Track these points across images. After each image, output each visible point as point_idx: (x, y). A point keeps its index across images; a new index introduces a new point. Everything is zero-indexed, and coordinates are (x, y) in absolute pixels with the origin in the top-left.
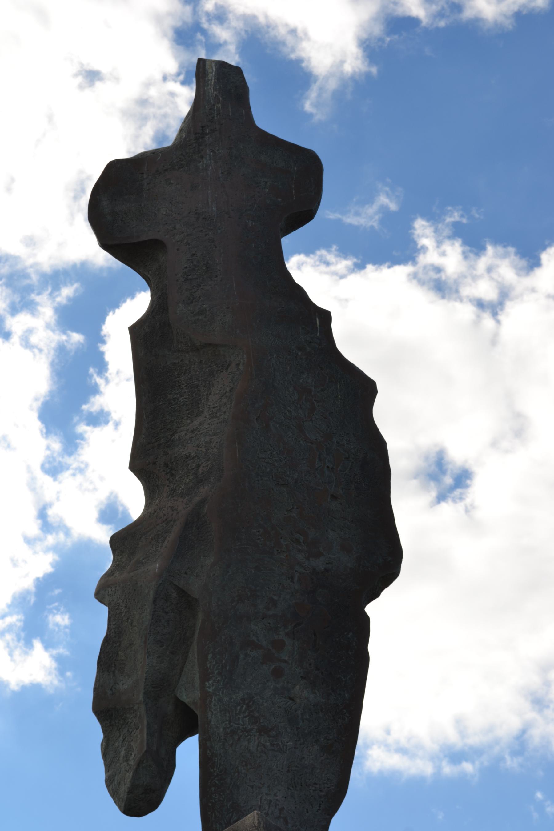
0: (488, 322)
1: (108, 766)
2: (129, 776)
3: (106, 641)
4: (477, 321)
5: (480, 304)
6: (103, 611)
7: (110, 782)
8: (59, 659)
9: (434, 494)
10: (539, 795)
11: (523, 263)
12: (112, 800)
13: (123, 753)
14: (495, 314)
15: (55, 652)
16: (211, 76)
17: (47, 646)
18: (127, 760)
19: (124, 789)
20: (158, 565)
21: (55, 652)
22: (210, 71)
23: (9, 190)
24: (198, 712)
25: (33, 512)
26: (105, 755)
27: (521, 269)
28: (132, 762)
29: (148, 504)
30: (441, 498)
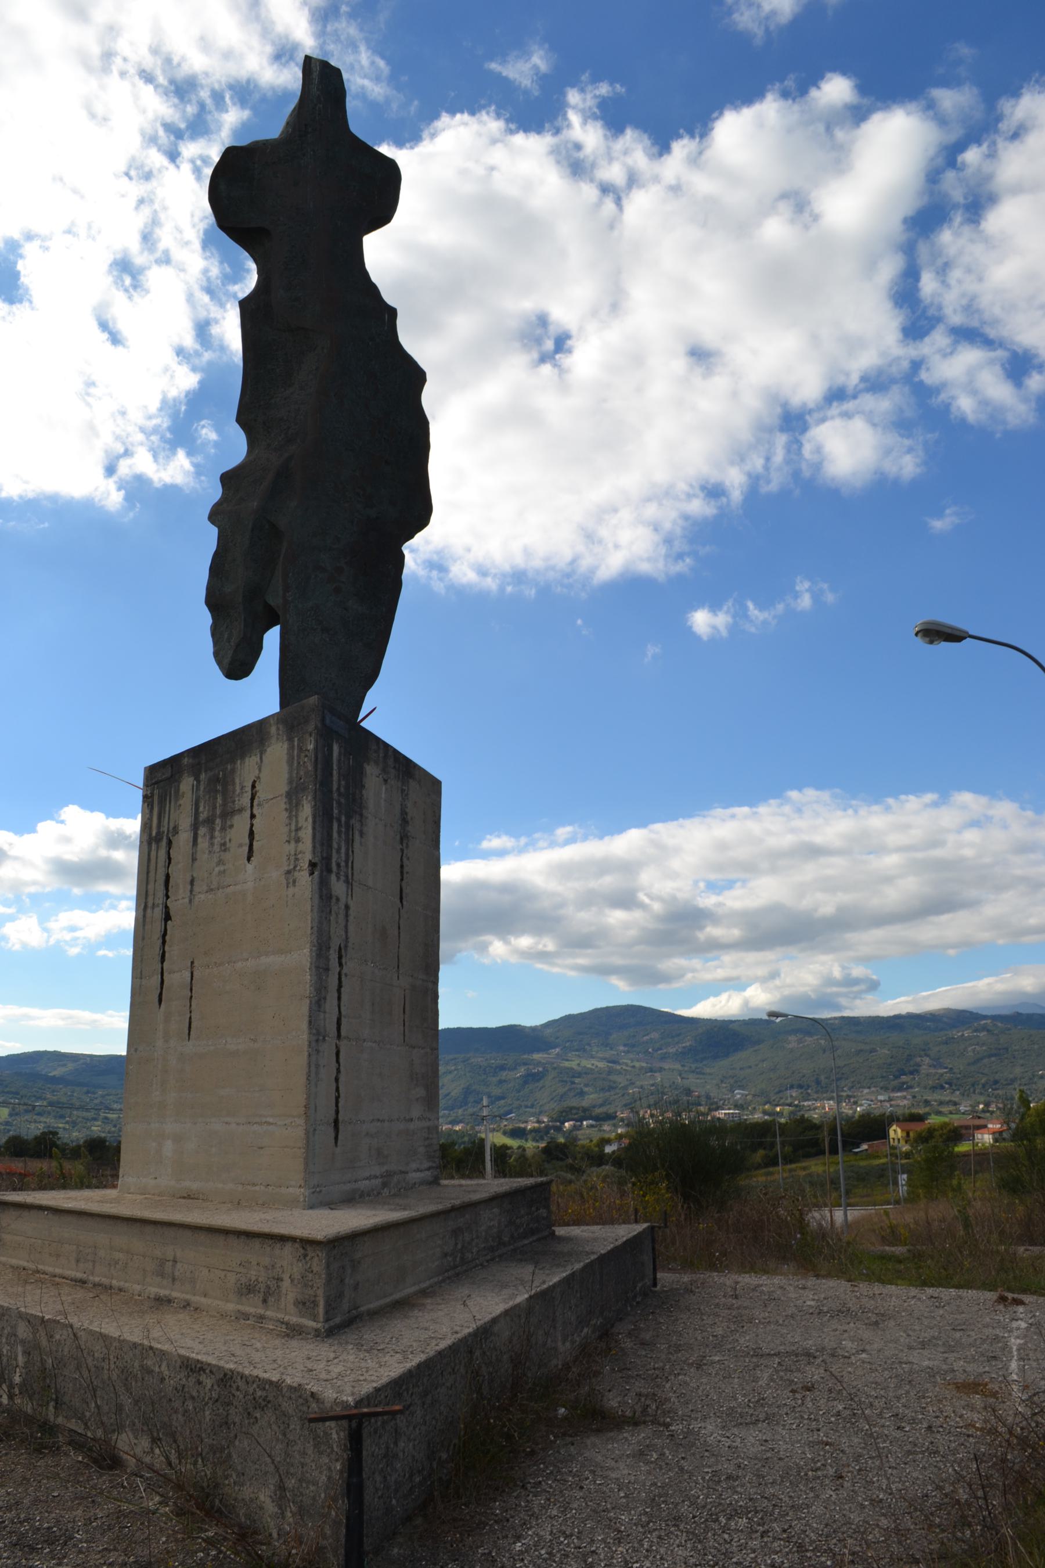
0: (609, 205)
1: (215, 644)
2: (230, 653)
3: (216, 556)
4: (599, 205)
5: (606, 189)
6: (214, 531)
7: (216, 654)
8: (196, 465)
9: (535, 355)
10: (579, 622)
11: (655, 150)
12: (217, 667)
13: (226, 636)
14: (618, 201)
15: (195, 460)
16: (315, 75)
17: (189, 454)
18: (229, 642)
19: (226, 661)
20: (255, 504)
21: (195, 460)
22: (314, 69)
23: (115, 339)
24: (280, 613)
25: (182, 298)
26: (213, 635)
27: (653, 155)
28: (232, 644)
29: (249, 451)
30: (543, 359)
